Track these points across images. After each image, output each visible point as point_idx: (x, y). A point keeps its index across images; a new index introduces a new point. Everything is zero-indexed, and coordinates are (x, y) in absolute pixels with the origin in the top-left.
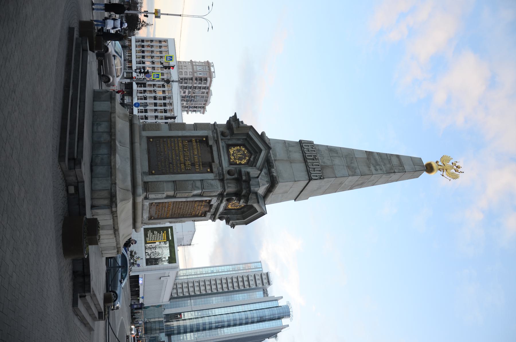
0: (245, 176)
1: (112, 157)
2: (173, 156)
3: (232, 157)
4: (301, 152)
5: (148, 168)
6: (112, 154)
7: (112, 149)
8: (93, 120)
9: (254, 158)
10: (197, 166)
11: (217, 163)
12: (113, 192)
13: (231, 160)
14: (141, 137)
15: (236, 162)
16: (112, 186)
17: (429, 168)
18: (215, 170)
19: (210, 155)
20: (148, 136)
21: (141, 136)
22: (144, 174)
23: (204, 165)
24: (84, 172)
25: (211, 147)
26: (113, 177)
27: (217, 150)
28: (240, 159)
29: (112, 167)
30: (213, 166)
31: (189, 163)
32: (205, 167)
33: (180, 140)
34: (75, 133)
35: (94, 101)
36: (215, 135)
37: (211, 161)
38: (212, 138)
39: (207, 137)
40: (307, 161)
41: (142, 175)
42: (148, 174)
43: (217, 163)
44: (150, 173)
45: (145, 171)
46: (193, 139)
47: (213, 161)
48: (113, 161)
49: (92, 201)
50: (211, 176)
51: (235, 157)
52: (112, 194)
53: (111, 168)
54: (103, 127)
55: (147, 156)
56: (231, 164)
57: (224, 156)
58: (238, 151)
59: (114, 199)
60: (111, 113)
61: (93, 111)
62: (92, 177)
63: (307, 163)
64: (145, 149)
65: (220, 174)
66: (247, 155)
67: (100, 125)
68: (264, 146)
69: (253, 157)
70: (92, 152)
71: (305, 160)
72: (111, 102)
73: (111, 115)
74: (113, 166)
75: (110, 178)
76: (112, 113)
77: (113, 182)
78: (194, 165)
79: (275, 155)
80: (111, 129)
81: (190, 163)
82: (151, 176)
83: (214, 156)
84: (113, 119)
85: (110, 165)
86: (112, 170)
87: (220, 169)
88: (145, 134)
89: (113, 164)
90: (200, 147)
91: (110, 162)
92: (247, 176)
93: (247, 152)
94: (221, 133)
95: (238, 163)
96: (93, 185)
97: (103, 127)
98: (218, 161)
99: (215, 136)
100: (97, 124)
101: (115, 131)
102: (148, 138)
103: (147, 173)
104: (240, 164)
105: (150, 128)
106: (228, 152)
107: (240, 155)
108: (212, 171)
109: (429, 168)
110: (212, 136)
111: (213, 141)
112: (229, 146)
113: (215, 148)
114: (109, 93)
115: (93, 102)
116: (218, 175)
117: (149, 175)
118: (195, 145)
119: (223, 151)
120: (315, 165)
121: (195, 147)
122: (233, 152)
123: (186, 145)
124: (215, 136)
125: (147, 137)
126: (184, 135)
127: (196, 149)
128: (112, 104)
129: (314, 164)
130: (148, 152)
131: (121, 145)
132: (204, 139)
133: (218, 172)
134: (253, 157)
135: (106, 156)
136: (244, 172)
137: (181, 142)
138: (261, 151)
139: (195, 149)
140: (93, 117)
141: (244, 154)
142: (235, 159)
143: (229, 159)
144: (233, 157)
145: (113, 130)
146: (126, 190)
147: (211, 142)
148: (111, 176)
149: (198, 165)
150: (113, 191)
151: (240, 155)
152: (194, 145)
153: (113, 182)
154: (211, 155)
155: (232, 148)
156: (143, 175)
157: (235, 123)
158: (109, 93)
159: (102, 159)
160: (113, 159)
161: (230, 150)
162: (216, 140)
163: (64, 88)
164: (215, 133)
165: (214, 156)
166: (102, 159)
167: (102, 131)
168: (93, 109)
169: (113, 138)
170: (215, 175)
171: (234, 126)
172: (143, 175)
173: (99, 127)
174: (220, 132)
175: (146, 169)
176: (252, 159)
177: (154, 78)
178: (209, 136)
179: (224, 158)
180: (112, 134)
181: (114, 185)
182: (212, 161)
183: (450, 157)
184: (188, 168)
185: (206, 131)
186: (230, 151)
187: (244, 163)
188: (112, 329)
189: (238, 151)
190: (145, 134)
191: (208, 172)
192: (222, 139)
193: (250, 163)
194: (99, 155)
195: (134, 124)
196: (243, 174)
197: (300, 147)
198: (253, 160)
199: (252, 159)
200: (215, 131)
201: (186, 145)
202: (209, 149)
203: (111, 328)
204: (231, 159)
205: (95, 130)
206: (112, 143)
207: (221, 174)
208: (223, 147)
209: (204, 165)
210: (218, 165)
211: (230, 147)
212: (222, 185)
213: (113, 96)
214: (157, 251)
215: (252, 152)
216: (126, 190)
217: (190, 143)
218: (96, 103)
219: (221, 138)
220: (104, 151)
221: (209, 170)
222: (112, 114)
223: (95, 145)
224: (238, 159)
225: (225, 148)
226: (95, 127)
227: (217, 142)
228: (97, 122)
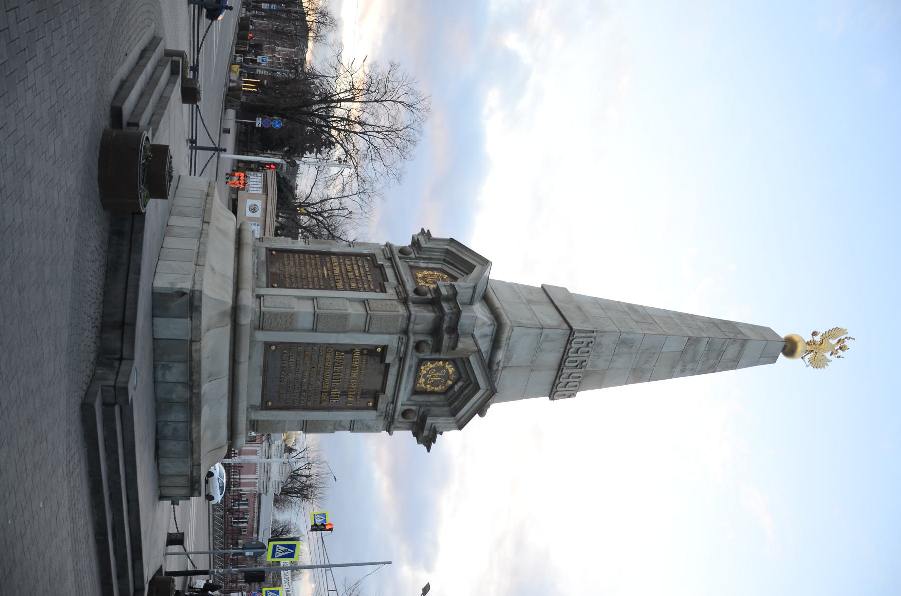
0: (430, 431)
1: (194, 425)
2: (310, 379)
3: (422, 380)
4: (562, 350)
5: (260, 399)
6: (194, 420)
7: (192, 407)
8: (154, 358)
9: (462, 389)
10: (351, 396)
11: (389, 395)
12: (194, 476)
14: (253, 343)
16: (194, 469)
17: (790, 348)
18: (382, 406)
19: (381, 378)
20: (266, 341)
21: (254, 341)
22: (252, 408)
23: (364, 394)
24: (146, 578)
25: (388, 366)
26: (195, 456)
27: (396, 374)
29: (194, 441)
30: (380, 400)
31: (338, 392)
32: (365, 398)
33: (330, 350)
34: (128, 577)
35: (153, 317)
36: (403, 347)
37: (379, 387)
38: (396, 350)
39: (385, 348)
40: (563, 369)
41: (247, 410)
42: (260, 409)
43: (389, 395)
44: (264, 407)
45: (253, 404)
46: (358, 350)
47: (383, 391)
48: (195, 430)
49: (160, 490)
50: (373, 414)
52: (194, 479)
53: (192, 442)
54: (176, 373)
55: (261, 379)
56: (416, 392)
57: (406, 383)
58: (439, 369)
59: (197, 486)
60: (191, 342)
61: (154, 339)
62: (159, 457)
63: (560, 374)
64: (259, 367)
65: (388, 416)
66: (452, 378)
67: (169, 368)
68: (486, 385)
69: (460, 384)
70: (157, 417)
71: (560, 366)
72: (191, 319)
73: (191, 346)
74: (195, 439)
75: (189, 459)
76: (193, 342)
77: (195, 464)
78: (347, 394)
79: (507, 359)
80: (191, 375)
81: (339, 393)
82: (264, 413)
83: (388, 383)
84: (195, 355)
85: (191, 437)
86: (194, 445)
87: (391, 408)
88: (262, 337)
89: (194, 436)
90: (367, 364)
91: (191, 433)
92: (431, 433)
94: (415, 344)
96: (160, 468)
97: (176, 373)
98: (392, 392)
99: (402, 350)
100: (163, 366)
101: (200, 378)
102: (268, 345)
103: (259, 407)
104: (433, 393)
105: (273, 323)
106: (418, 370)
107: (439, 377)
108: (375, 407)
109: (790, 348)
110: (396, 346)
111: (395, 356)
112: (421, 362)
113: (393, 371)
114: (186, 298)
115: (152, 320)
116: (384, 414)
117: (262, 410)
118: (357, 361)
119: (409, 375)
121: (356, 364)
123: (340, 360)
124: (402, 350)
125: (265, 342)
126: (339, 343)
127: (357, 368)
128: (194, 322)
130: (264, 371)
131: (210, 382)
132: (379, 350)
133: (385, 410)
134: (460, 384)
135: (181, 425)
136: (430, 425)
138: (477, 388)
139: (356, 367)
140: (154, 350)
141: (447, 377)
142: (426, 384)
145: (195, 378)
146: (217, 449)
147: (389, 359)
148: (192, 455)
149: (353, 395)
150: (195, 474)
152: (355, 361)
153: (195, 464)
154: (384, 378)
155: (429, 364)
156: (250, 410)
157: (450, 338)
158: (186, 296)
159: (175, 430)
160: (195, 428)
161: (423, 368)
162: (401, 358)
163: (95, 536)
164: (404, 344)
165: (388, 383)
166: (175, 430)
167: (174, 381)
168: (153, 335)
169: (195, 391)
170: (378, 414)
171: (444, 344)
172: (250, 410)
173: (167, 372)
174: (414, 342)
175: (257, 401)
176: (456, 388)
177: (273, 557)
178: (389, 347)
179: (406, 388)
180: (193, 386)
181: (196, 467)
182: (382, 390)
183: (846, 330)
184: (334, 401)
185: (387, 337)
186: (423, 371)
188: (201, 118)
189: (439, 369)
190: (262, 337)
191: (368, 408)
193: (450, 394)
194: (169, 423)
195: (241, 325)
196: (426, 428)
197: (566, 342)
198: (458, 391)
199: (456, 388)
200: (404, 340)
202: (383, 367)
203: (201, 118)
205: (160, 379)
206: (194, 400)
207: (390, 415)
208: (411, 367)
209: (364, 394)
210: (390, 400)
211: (425, 363)
212: (386, 426)
213: (196, 304)
214: (287, 128)
215: (463, 376)
216: (217, 449)
217: (349, 356)
218: (158, 321)
220: (177, 416)
221: (371, 404)
222: (194, 344)
223: (160, 406)
224: (433, 385)
225: (413, 369)
226: (159, 374)
227: (402, 361)
228: (163, 363)
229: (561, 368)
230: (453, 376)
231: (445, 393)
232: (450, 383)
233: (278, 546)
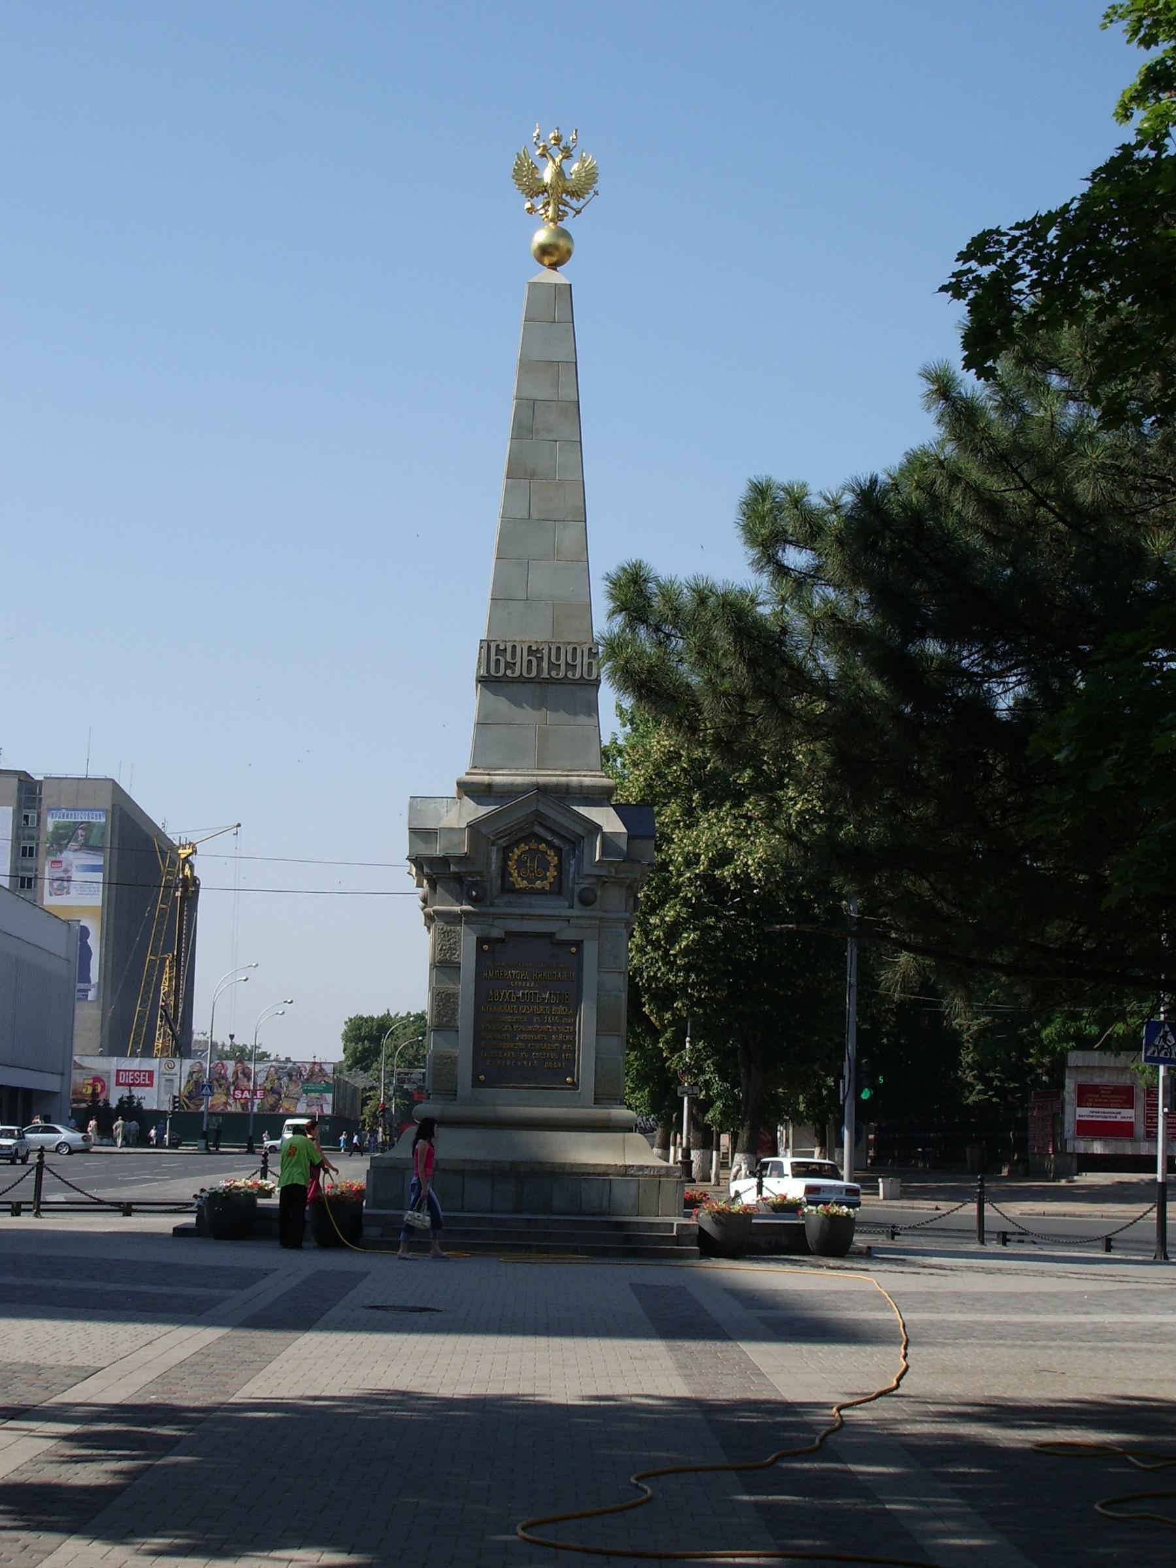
13: (547, 888)
15: (554, 877)
28: (545, 866)
40: (543, 678)
51: (539, 879)
58: (520, 863)
93: (525, 845)
95: (555, 873)
102: (476, 1083)
104: (559, 867)
107: (532, 862)
112: (508, 889)
120: (558, 659)
122: (523, 879)
123: (500, 995)
129: (553, 659)
132: (486, 947)
137: (493, 1007)
139: (512, 974)
142: (544, 878)
143: (541, 892)
144: (538, 882)
147: (497, 933)
151: (532, 862)
155: (511, 879)
161: (517, 886)
187: (556, 858)
192: (492, 905)
201: (502, 994)
204: (543, 888)
210: (565, 924)
219: (488, 903)
221: (574, 950)
229: (541, 680)
230: (531, 844)
231: (559, 851)
232: (543, 846)
233: (1148, 1054)
